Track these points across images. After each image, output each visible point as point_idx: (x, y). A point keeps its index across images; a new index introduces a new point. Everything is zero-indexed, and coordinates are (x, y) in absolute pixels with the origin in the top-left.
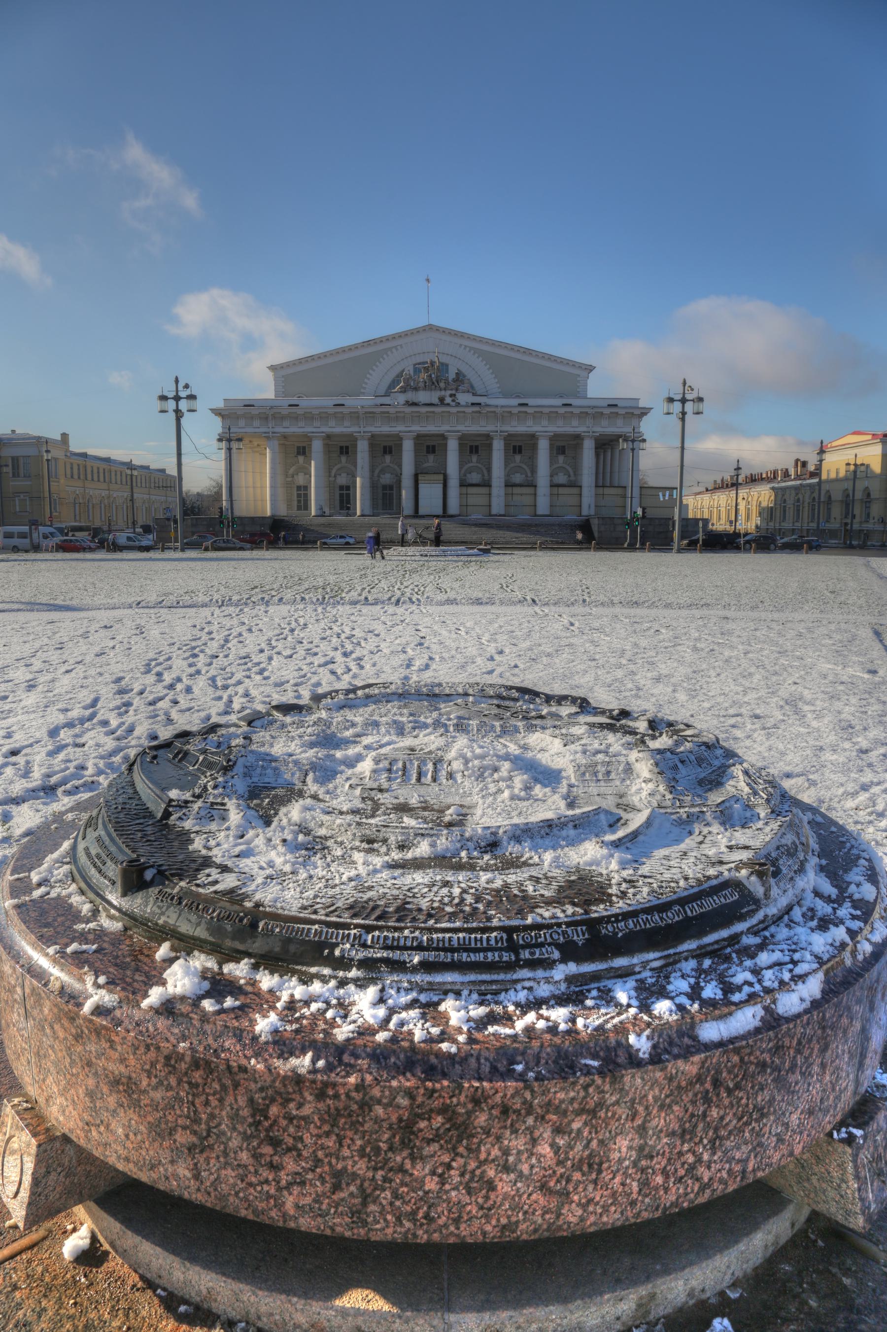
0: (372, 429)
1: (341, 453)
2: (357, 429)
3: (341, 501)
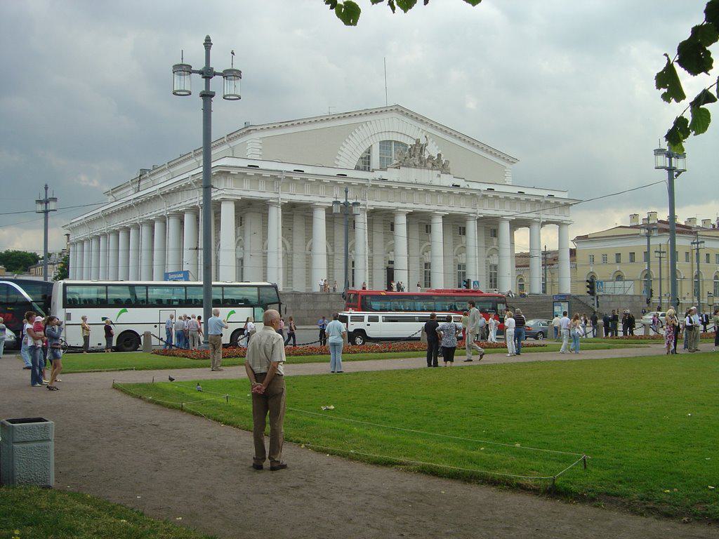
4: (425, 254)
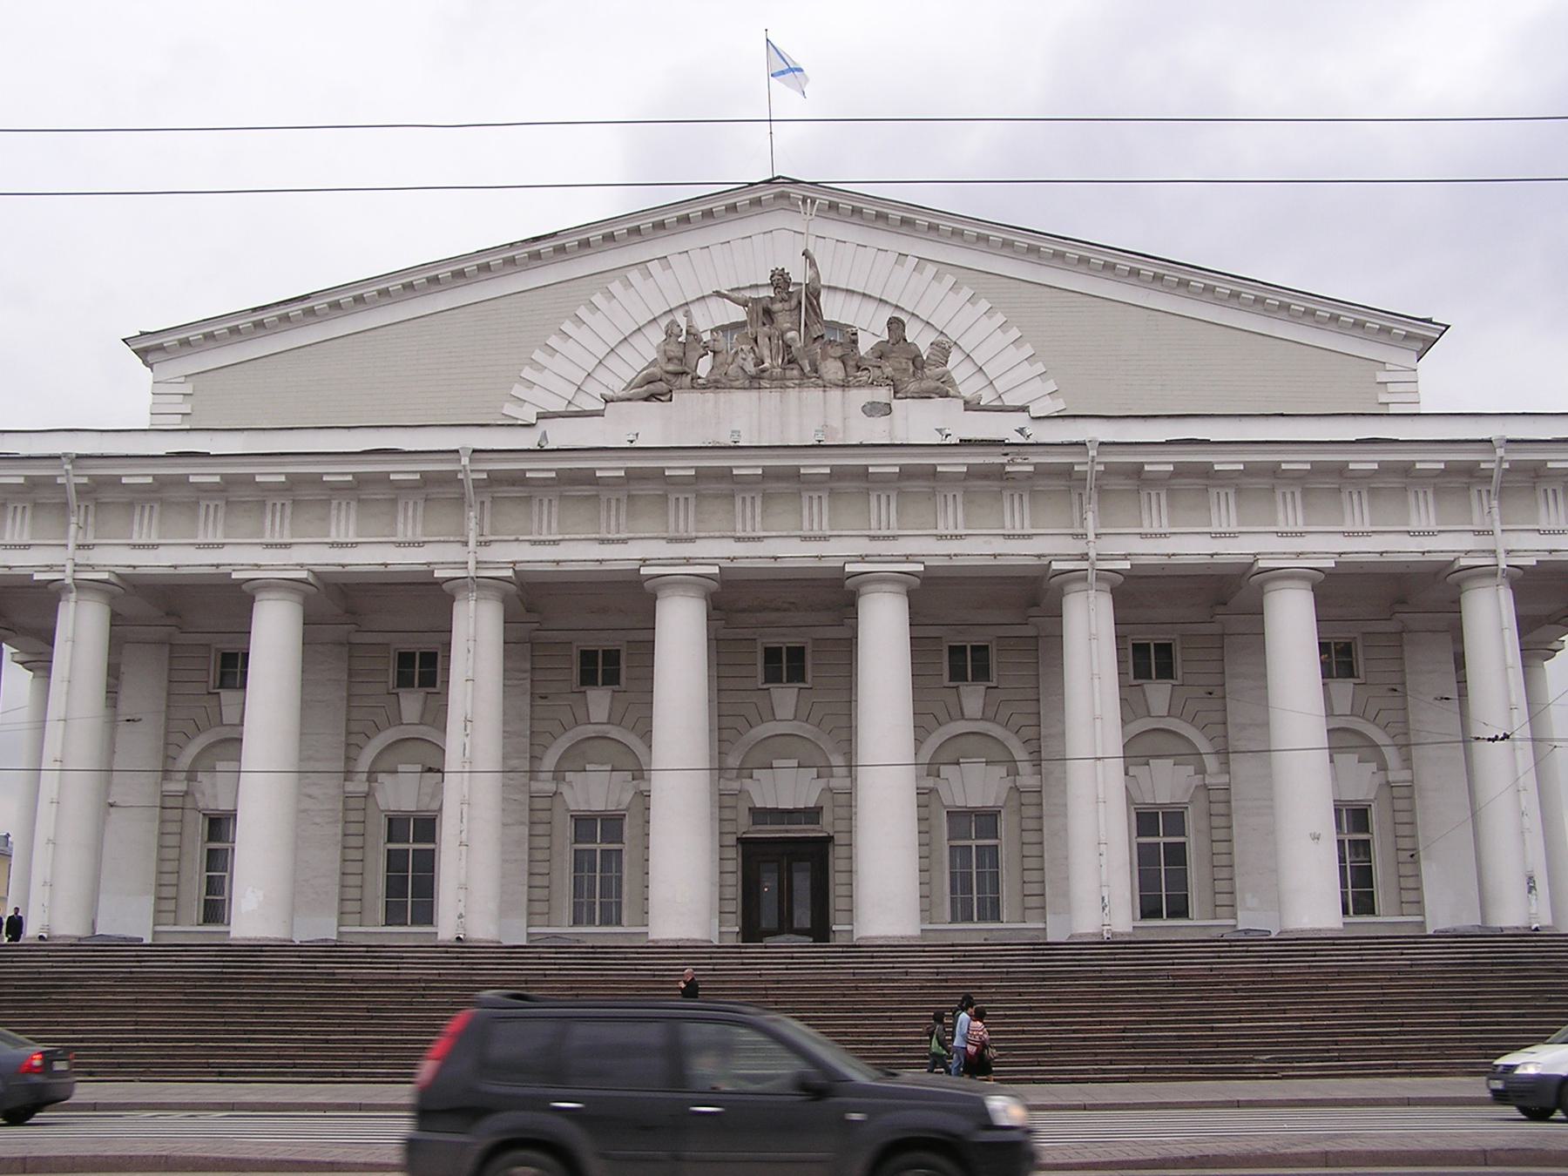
1: (404, 681)
3: (395, 887)
4: (945, 771)
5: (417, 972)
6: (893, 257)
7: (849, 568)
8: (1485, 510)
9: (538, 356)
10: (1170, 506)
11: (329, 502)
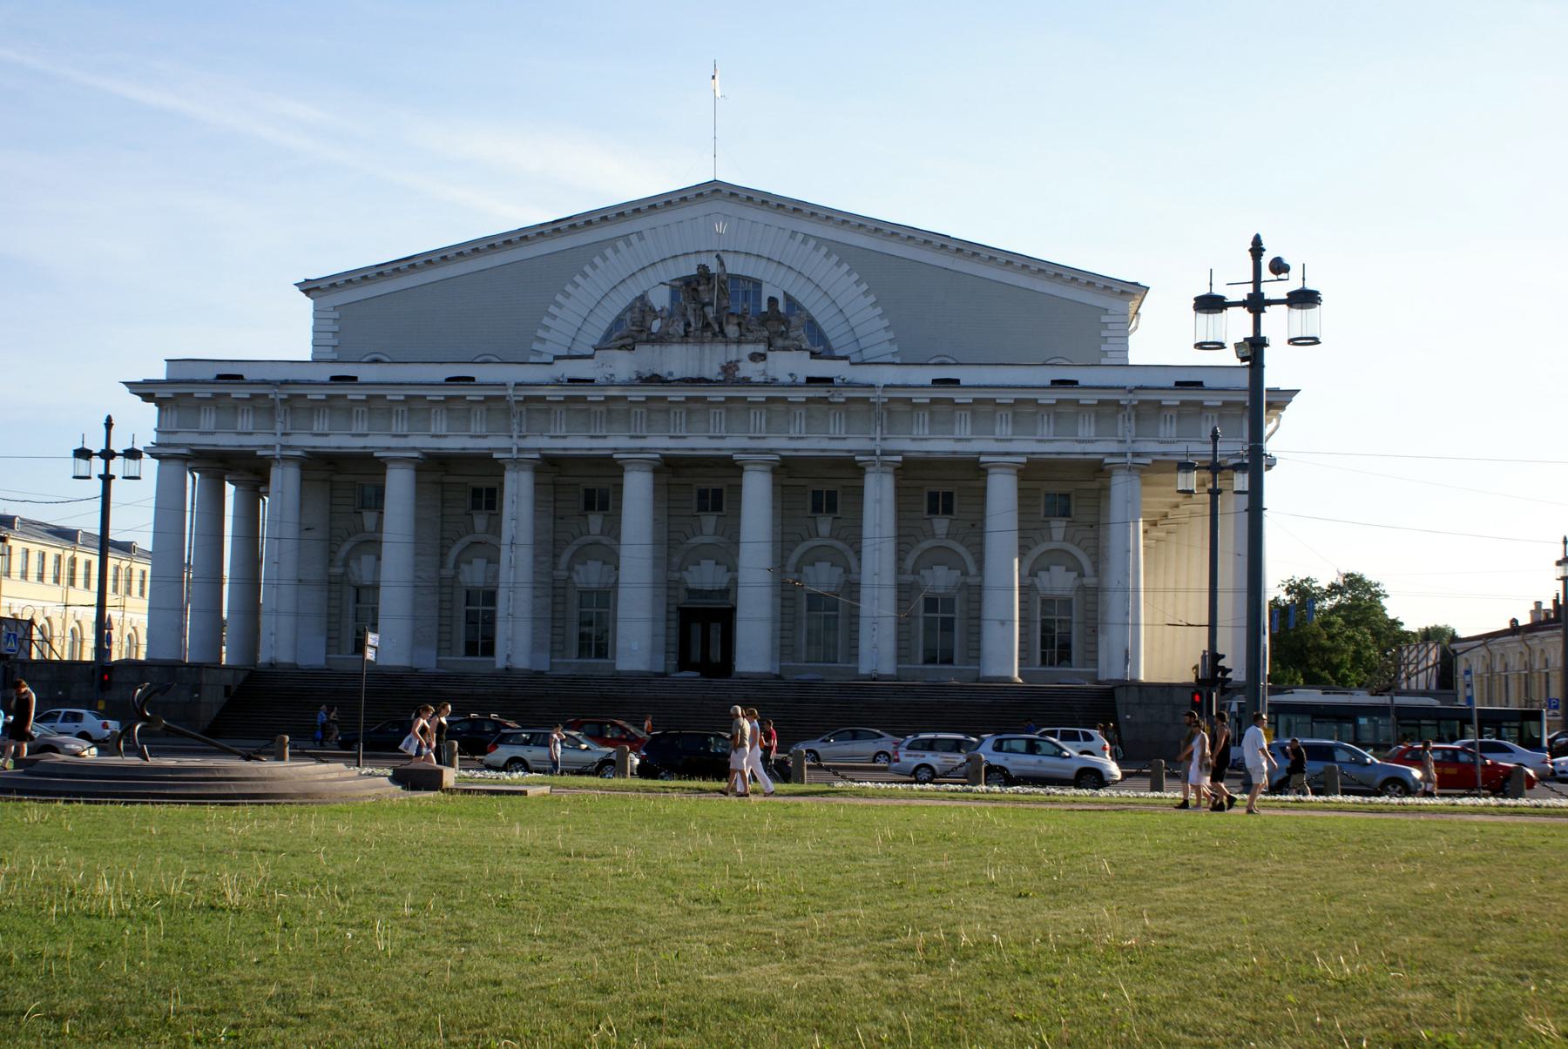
0: (544, 443)
2: (503, 442)
4: (807, 569)
5: (482, 691)
6: (788, 233)
7: (736, 457)
8: (1126, 428)
9: (559, 298)
10: (931, 421)
11: (429, 410)
